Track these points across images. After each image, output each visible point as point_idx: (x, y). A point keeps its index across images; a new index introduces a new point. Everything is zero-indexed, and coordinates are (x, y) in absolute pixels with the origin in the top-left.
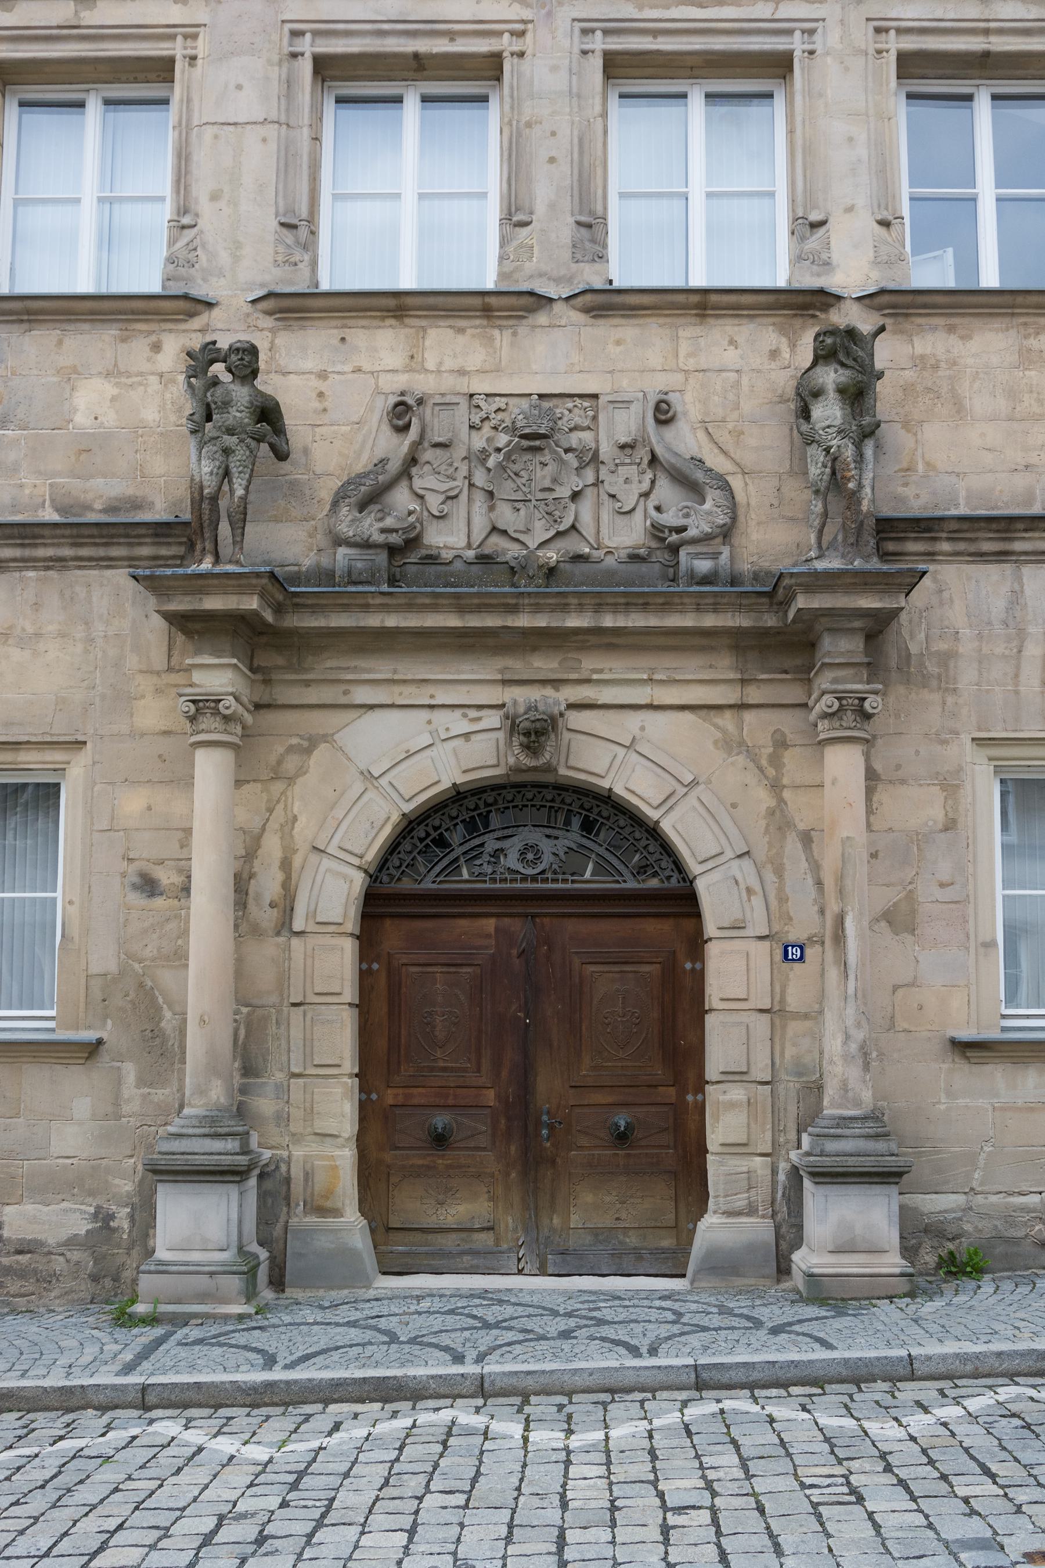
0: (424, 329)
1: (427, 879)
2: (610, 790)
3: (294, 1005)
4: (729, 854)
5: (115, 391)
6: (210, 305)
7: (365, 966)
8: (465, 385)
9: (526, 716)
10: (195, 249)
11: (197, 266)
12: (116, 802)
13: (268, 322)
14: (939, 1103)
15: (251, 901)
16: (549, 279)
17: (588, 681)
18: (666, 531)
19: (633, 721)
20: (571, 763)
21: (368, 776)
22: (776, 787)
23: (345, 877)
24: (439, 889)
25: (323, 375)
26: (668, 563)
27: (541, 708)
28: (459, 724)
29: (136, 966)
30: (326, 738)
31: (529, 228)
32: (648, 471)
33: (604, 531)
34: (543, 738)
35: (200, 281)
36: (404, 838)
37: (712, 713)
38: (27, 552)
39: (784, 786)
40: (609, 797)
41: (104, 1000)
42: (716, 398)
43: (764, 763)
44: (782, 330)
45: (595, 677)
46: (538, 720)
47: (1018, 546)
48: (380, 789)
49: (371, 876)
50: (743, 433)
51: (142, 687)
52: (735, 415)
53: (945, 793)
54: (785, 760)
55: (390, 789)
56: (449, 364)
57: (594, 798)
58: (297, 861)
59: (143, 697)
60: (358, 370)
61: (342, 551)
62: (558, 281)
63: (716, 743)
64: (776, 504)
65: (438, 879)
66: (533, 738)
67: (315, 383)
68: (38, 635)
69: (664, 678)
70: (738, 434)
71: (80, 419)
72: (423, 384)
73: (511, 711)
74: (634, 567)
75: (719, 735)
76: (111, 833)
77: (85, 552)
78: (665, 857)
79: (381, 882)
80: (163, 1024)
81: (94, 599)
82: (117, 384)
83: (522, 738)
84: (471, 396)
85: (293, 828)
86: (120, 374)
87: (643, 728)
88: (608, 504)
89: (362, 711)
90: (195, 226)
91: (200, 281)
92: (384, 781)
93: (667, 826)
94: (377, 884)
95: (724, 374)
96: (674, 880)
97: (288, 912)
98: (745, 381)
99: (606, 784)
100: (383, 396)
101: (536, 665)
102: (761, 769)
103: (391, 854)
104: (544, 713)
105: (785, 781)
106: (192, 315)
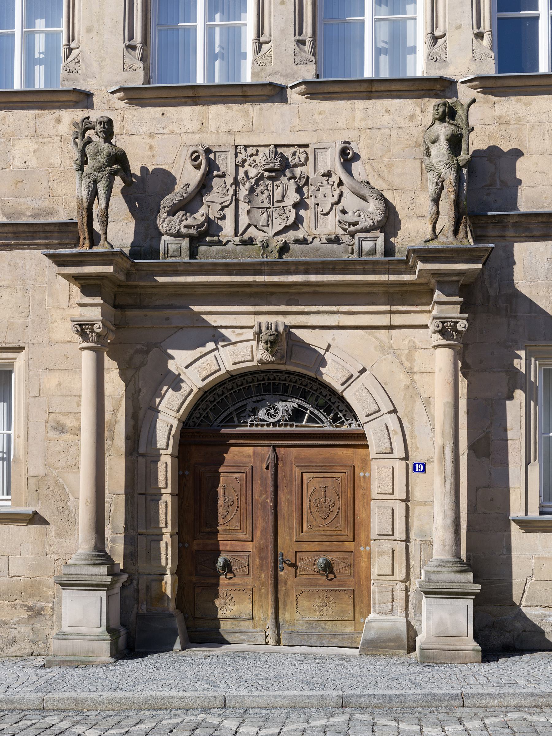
3: (140, 494)
7: (181, 473)
8: (231, 140)
10: (79, 62)
11: (80, 72)
12: (42, 381)
13: (122, 104)
14: (503, 554)
15: (115, 436)
16: (281, 75)
18: (347, 224)
22: (410, 373)
25: (152, 135)
26: (349, 243)
29: (54, 472)
31: (269, 44)
32: (337, 189)
35: (81, 81)
39: (414, 373)
41: (37, 491)
42: (377, 145)
43: (403, 358)
50: (393, 165)
51: (54, 316)
52: (388, 155)
53: (508, 377)
54: (416, 358)
56: (223, 128)
58: (141, 414)
59: (55, 322)
62: (286, 76)
63: (375, 347)
64: (411, 208)
65: (221, 424)
67: (148, 140)
70: (389, 167)
71: (17, 163)
75: (377, 343)
76: (39, 398)
79: (189, 426)
80: (69, 504)
81: (28, 267)
84: (236, 146)
85: (139, 395)
87: (334, 339)
90: (79, 48)
91: (81, 81)
95: (383, 131)
97: (136, 442)
98: (394, 134)
100: (186, 148)
102: (401, 363)
105: (415, 370)
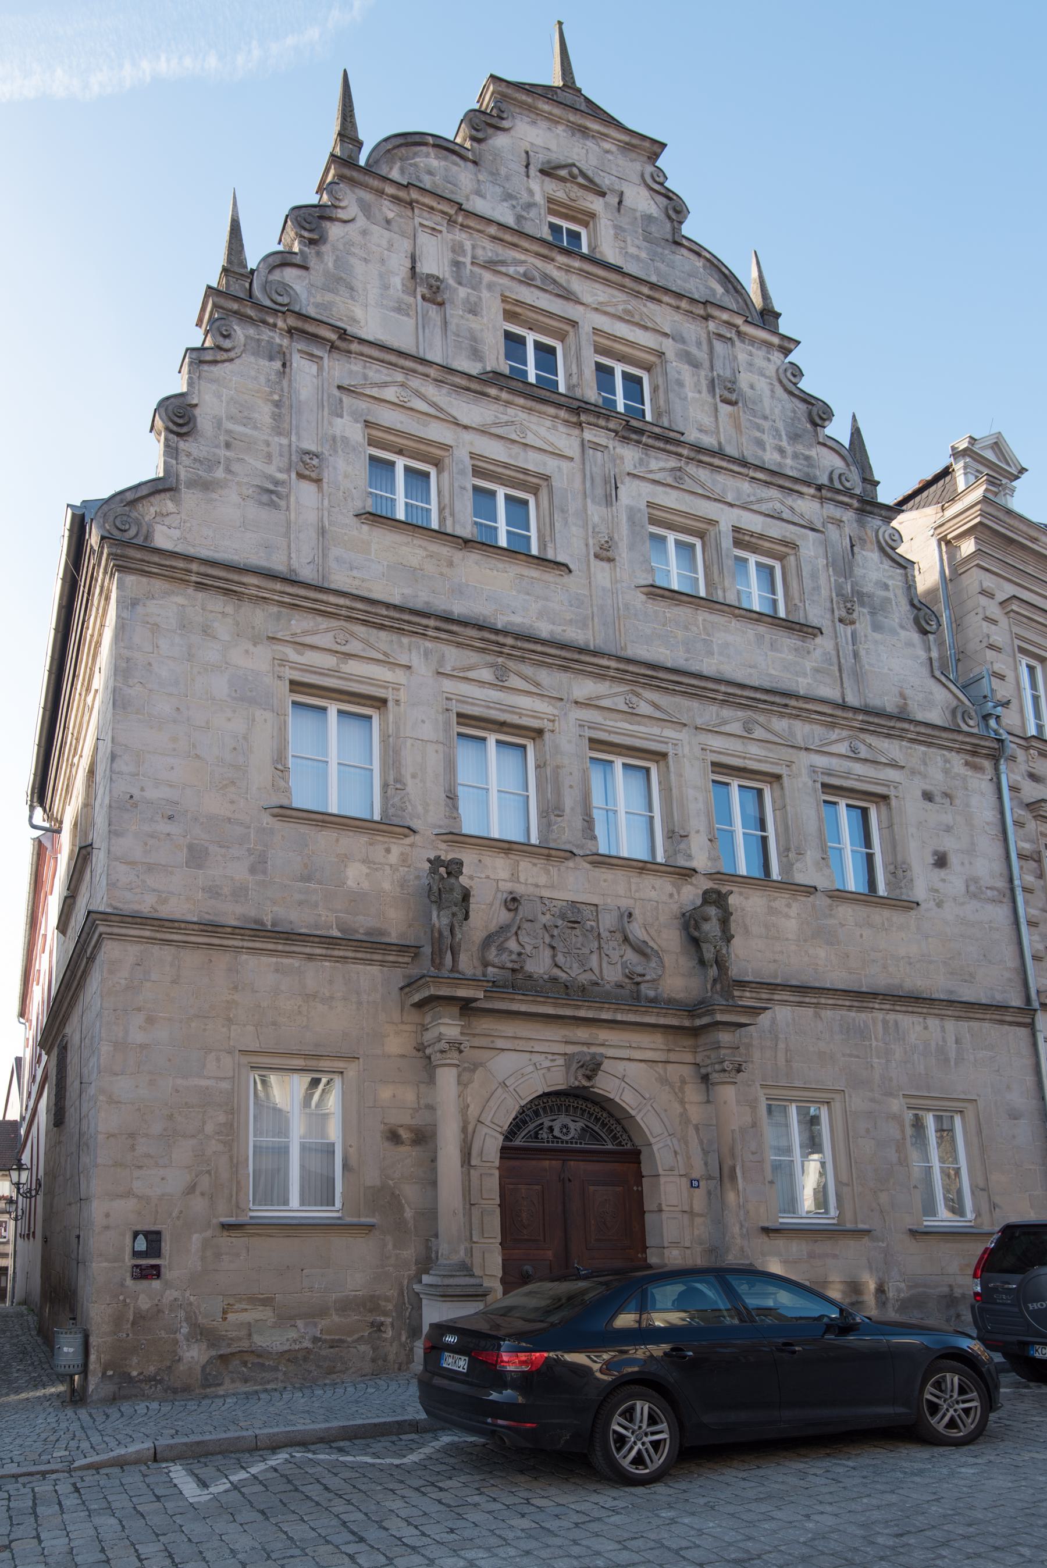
0: (518, 862)
5: (368, 871)
6: (414, 832)
17: (603, 1045)
23: (496, 1138)
30: (481, 1064)
33: (605, 972)
38: (329, 952)
44: (674, 884)
47: (776, 997)
58: (470, 1128)
60: (488, 877)
61: (490, 969)
68: (332, 998)
71: (350, 883)
72: (520, 889)
74: (619, 991)
77: (359, 955)
82: (369, 867)
86: (370, 862)
88: (605, 958)
106: (406, 836)
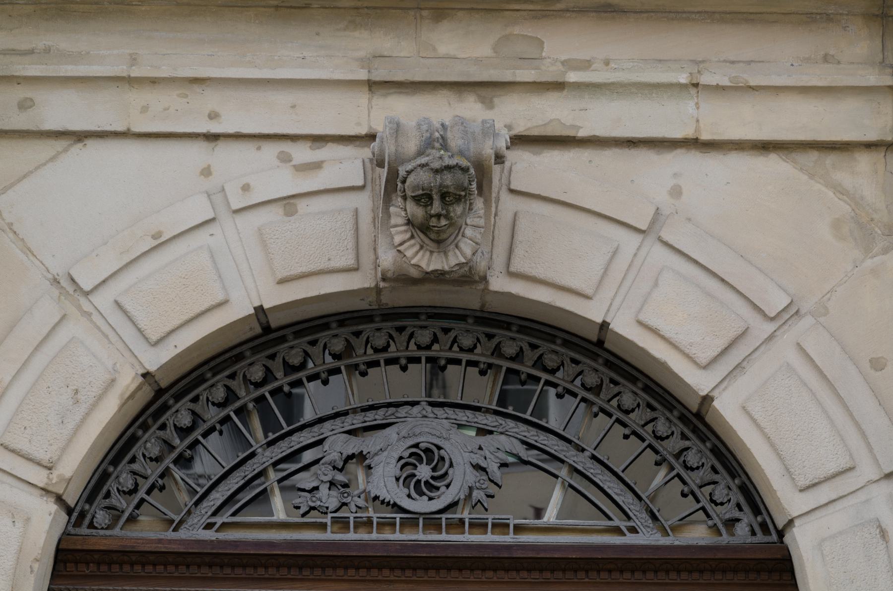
1: (193, 520)
2: (604, 325)
4: (867, 471)
9: (423, 160)
17: (559, 86)
19: (656, 174)
20: (517, 265)
21: (69, 287)
23: (13, 512)
24: (219, 541)
27: (455, 141)
28: (268, 174)
34: (458, 209)
36: (145, 427)
37: (830, 159)
40: (600, 343)
45: (573, 77)
46: (449, 168)
48: (96, 317)
49: (69, 511)
55: (116, 319)
57: (566, 343)
63: (836, 225)
65: (219, 520)
66: (437, 207)
69: (726, 82)
73: (390, 149)
75: (844, 208)
78: (723, 477)
79: (91, 526)
83: (411, 206)
87: (676, 192)
89: (60, 144)
92: (103, 300)
93: (730, 410)
94: (84, 530)
96: (742, 530)
99: (594, 312)
101: (443, 49)
103: (115, 462)
104: (461, 153)
